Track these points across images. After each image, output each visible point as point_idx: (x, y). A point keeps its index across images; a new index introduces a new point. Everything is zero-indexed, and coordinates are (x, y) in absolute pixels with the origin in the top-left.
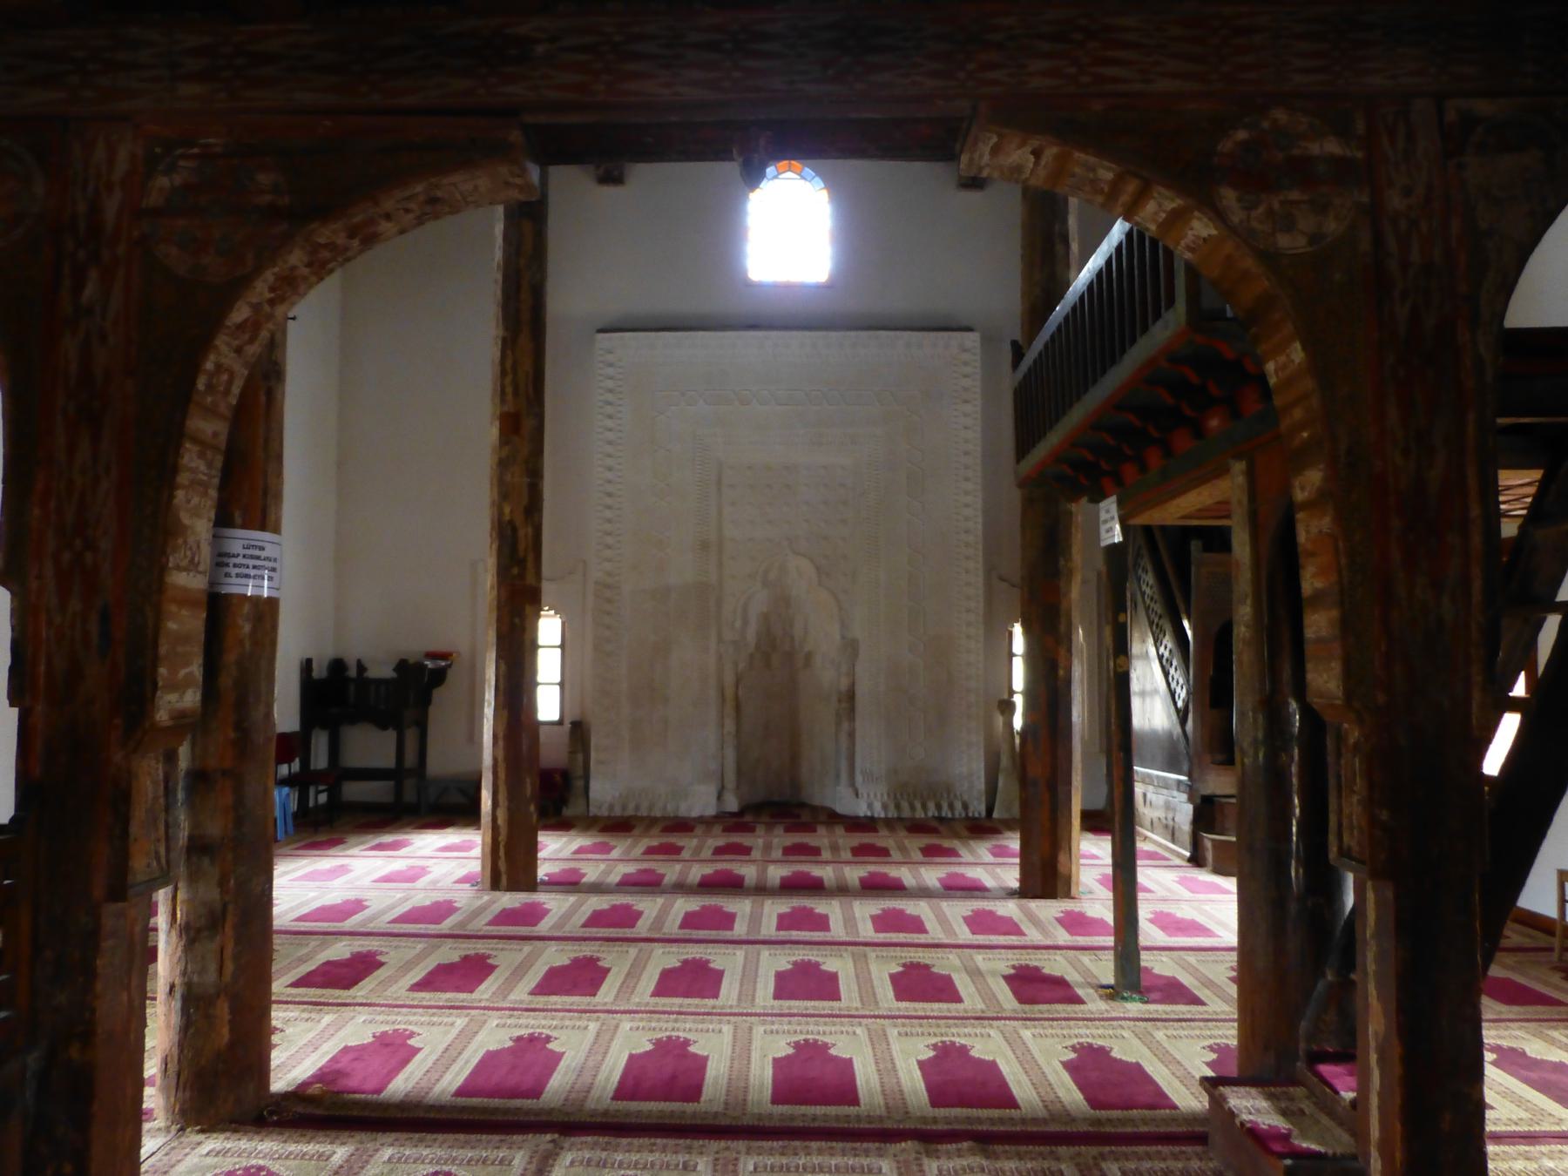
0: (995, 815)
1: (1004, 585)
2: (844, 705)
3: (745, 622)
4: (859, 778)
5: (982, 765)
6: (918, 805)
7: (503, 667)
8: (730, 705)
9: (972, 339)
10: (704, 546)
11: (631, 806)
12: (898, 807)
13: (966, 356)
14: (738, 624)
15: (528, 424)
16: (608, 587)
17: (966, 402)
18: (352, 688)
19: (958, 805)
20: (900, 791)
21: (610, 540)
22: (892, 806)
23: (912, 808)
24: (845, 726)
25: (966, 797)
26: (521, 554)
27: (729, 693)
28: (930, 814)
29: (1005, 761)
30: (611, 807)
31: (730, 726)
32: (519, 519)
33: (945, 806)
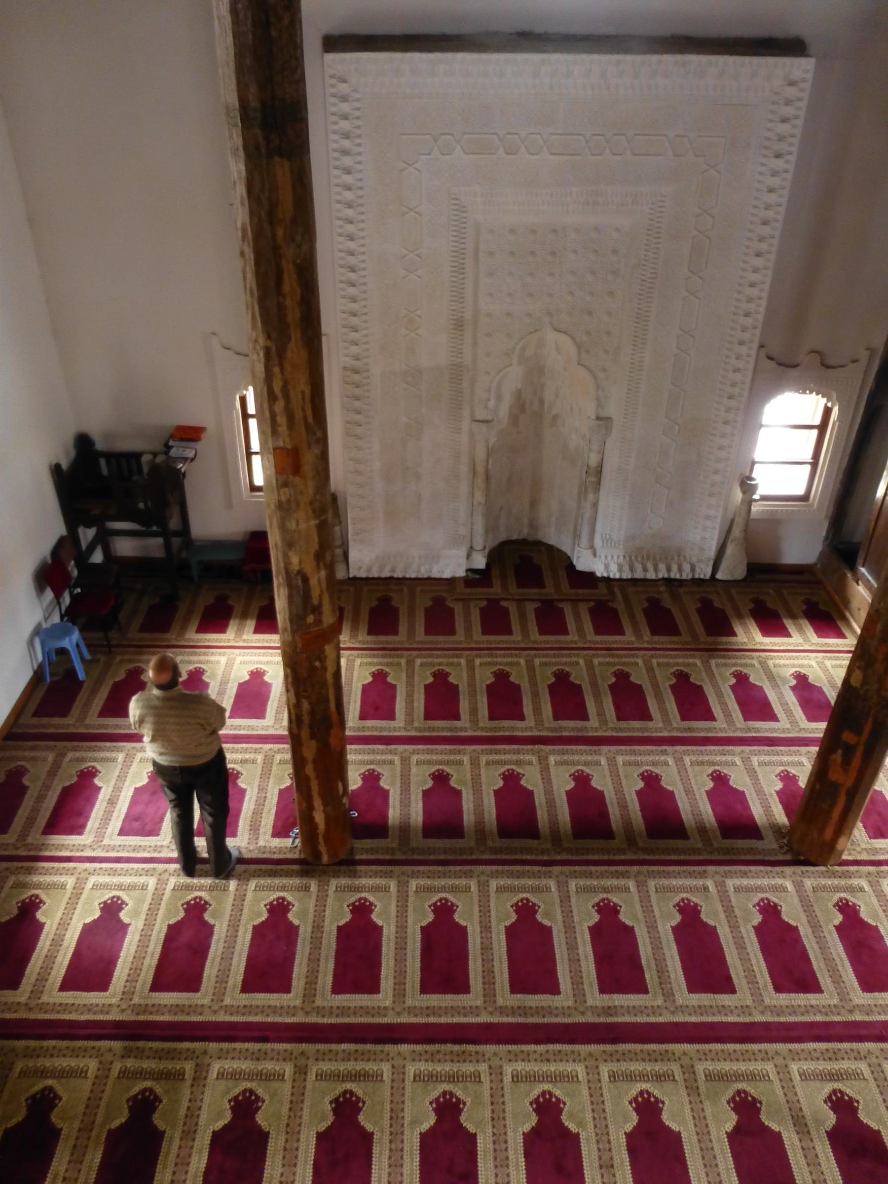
0: (719, 576)
1: (772, 364)
2: (593, 479)
3: (499, 398)
4: (598, 542)
5: (716, 536)
6: (650, 567)
7: (305, 705)
8: (480, 480)
9: (801, 68)
10: (459, 325)
11: (388, 568)
12: (632, 569)
13: (791, 92)
14: (491, 404)
15: (308, 458)
16: (356, 371)
17: (778, 156)
18: (103, 462)
19: (687, 568)
20: (634, 554)
21: (355, 321)
22: (626, 568)
23: (645, 570)
24: (591, 497)
25: (694, 560)
26: (315, 601)
27: (480, 469)
28: (660, 576)
29: (737, 532)
30: (369, 569)
31: (479, 497)
32: (309, 567)
33: (675, 568)
